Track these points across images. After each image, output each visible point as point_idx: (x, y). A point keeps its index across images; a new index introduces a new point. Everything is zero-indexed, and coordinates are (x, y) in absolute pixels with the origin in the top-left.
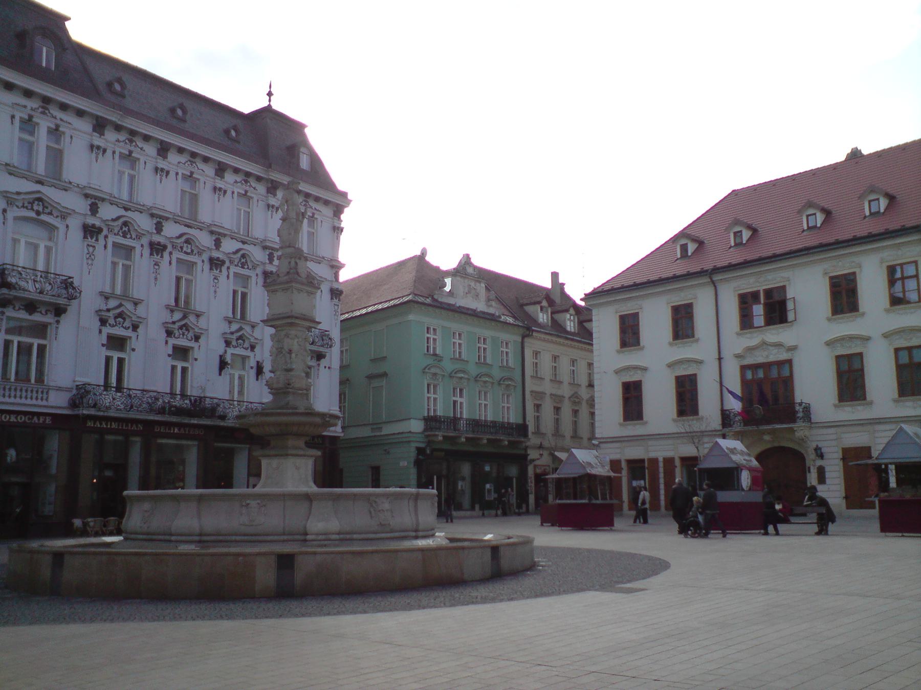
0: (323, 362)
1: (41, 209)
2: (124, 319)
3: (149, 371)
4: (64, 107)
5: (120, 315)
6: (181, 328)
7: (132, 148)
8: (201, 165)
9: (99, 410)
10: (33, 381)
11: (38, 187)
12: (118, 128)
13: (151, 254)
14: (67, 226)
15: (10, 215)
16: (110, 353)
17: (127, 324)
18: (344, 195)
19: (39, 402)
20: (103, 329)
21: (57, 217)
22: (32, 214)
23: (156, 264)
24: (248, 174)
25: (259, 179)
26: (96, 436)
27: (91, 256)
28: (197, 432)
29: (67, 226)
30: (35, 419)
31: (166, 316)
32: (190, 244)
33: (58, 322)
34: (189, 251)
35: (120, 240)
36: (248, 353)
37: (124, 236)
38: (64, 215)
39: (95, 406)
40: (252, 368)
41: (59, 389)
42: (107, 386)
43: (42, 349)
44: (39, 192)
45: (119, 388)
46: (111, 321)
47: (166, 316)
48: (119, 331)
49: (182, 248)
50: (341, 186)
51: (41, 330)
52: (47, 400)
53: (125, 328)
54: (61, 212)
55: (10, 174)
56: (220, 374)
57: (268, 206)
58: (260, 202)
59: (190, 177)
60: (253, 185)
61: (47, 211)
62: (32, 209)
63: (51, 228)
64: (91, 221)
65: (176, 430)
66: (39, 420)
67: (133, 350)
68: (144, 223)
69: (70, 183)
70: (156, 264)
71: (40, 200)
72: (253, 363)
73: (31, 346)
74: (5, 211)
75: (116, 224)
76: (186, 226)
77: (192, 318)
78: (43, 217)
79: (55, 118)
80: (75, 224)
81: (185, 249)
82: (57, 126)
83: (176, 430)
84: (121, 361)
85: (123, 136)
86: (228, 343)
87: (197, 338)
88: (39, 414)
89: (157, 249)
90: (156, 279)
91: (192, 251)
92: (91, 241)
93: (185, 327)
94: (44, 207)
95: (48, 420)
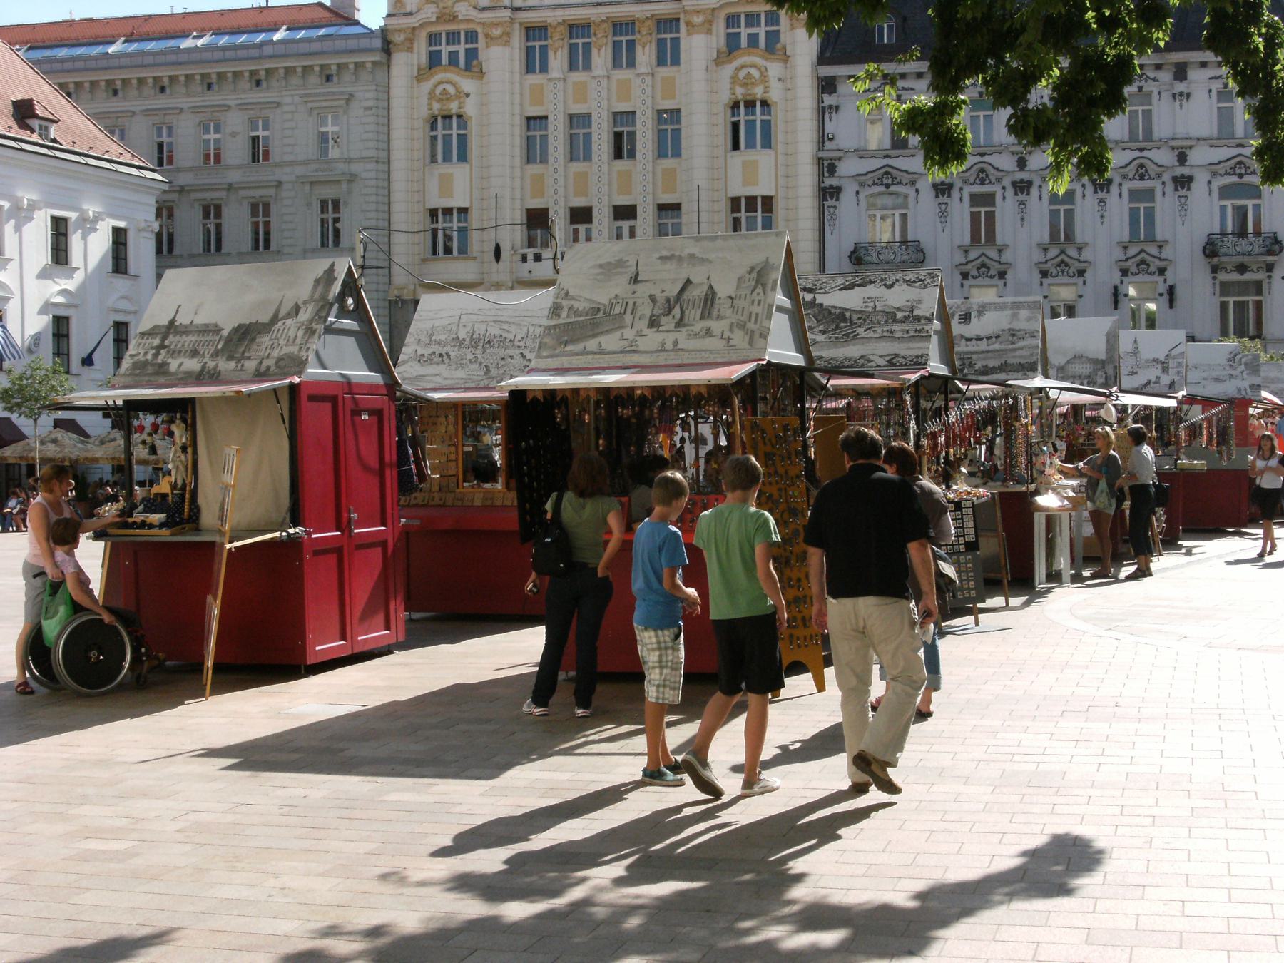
4: (903, 76)
5: (983, 265)
6: (1059, 265)
11: (887, 161)
14: (917, 191)
15: (862, 196)
17: (992, 272)
20: (965, 282)
22: (882, 189)
23: (1022, 203)
25: (1158, 67)
27: (943, 214)
29: (917, 191)
31: (1038, 256)
35: (978, 189)
36: (1156, 278)
37: (982, 183)
40: (1161, 295)
46: (974, 273)
47: (1038, 256)
56: (1116, 308)
57: (1174, 95)
58: (1163, 94)
60: (1151, 75)
71: (887, 173)
72: (1162, 288)
75: (967, 174)
77: (1072, 252)
78: (893, 189)
86: (1125, 272)
89: (1022, 187)
90: (1022, 219)
92: (942, 199)
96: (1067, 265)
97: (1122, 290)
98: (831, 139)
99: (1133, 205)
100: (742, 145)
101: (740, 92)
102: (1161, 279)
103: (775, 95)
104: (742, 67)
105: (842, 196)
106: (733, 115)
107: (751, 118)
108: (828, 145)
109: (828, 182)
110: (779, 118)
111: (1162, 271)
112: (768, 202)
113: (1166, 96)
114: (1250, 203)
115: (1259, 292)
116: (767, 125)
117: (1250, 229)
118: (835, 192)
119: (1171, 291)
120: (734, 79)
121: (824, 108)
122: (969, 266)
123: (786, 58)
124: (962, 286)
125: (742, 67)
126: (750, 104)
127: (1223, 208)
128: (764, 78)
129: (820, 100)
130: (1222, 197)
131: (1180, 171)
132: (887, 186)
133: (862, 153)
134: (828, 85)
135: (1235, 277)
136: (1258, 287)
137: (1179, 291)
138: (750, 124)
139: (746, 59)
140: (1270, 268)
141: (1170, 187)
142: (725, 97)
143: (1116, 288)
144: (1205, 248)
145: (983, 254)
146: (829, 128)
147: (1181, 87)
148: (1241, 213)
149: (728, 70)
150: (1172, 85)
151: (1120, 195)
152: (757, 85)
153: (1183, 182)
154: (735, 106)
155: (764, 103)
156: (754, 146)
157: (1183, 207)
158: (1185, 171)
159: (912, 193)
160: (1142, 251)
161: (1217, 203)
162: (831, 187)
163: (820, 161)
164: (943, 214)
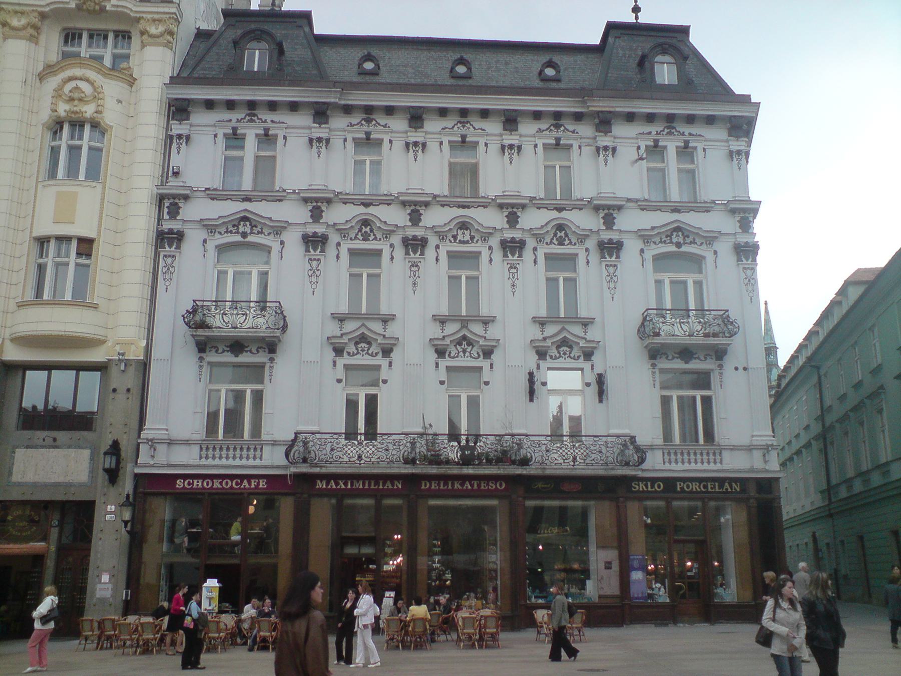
0: (729, 363)
1: (248, 229)
2: (369, 343)
3: (416, 406)
4: (273, 106)
7: (371, 128)
8: (479, 124)
9: (316, 466)
10: (246, 436)
12: (348, 110)
13: (407, 253)
14: (282, 243)
15: (211, 246)
16: (352, 391)
18: (745, 100)
19: (251, 462)
21: (269, 234)
22: (238, 238)
23: (415, 265)
24: (558, 116)
25: (578, 117)
26: (334, 501)
27: (314, 273)
28: (492, 486)
30: (245, 482)
32: (467, 229)
33: (272, 360)
34: (467, 238)
35: (360, 245)
38: (278, 229)
39: (305, 460)
40: (588, 385)
41: (275, 443)
42: (351, 434)
43: (258, 397)
44: (246, 210)
45: (371, 433)
48: (363, 360)
49: (455, 237)
50: (738, 89)
51: (256, 372)
52: (261, 458)
53: (372, 355)
54: (273, 227)
55: (213, 199)
56: (531, 400)
59: (463, 144)
60: (571, 128)
61: (255, 230)
62: (238, 233)
63: (268, 250)
64: (311, 229)
65: (457, 486)
66: (250, 485)
67: (385, 382)
68: (396, 216)
69: (284, 191)
70: (415, 265)
71: (245, 219)
72: (591, 378)
73: (243, 392)
74: (205, 241)
76: (459, 207)
79: (265, 121)
80: (293, 238)
81: (459, 237)
82: (266, 130)
83: (457, 486)
84: (372, 402)
85: (356, 119)
86: (542, 354)
87: (488, 353)
88: (249, 477)
91: (472, 238)
93: (464, 341)
94: (252, 227)
95: (262, 484)
96: (470, 344)
97: (538, 378)
98: (176, 174)
99: (551, 274)
100: (61, 173)
101: (63, 109)
102: (587, 366)
103: (110, 117)
104: (71, 79)
105: (185, 246)
106: (54, 139)
107: (76, 142)
108: (172, 181)
109: (167, 226)
110: (113, 144)
111: (588, 355)
112: (86, 246)
113: (587, 151)
114: (690, 279)
115: (708, 386)
116: (96, 151)
117: (692, 306)
118: (177, 238)
119: (601, 380)
120: (58, 93)
121: (171, 137)
122: (345, 339)
123: (131, 82)
124: (335, 363)
125: (71, 79)
126: (77, 124)
127: (659, 283)
128: (97, 96)
129: (167, 128)
130: (656, 270)
131: (606, 236)
132: (244, 235)
133: (213, 195)
134: (179, 110)
135: (678, 364)
136: (702, 380)
137: (611, 382)
138: (74, 151)
139: (78, 72)
140: (720, 354)
141: (594, 257)
142: (45, 115)
143: (531, 374)
144: (639, 331)
145: (363, 325)
146: (176, 161)
147: (604, 141)
148: (679, 286)
149: (53, 82)
150: (595, 138)
151: (535, 262)
152: (87, 103)
153: (610, 249)
154: (56, 127)
155: (95, 125)
156: (76, 175)
157: (612, 278)
158: (615, 236)
159: (276, 246)
160: (563, 329)
161: (651, 277)
162: (171, 231)
163: (161, 198)
164: (314, 273)
